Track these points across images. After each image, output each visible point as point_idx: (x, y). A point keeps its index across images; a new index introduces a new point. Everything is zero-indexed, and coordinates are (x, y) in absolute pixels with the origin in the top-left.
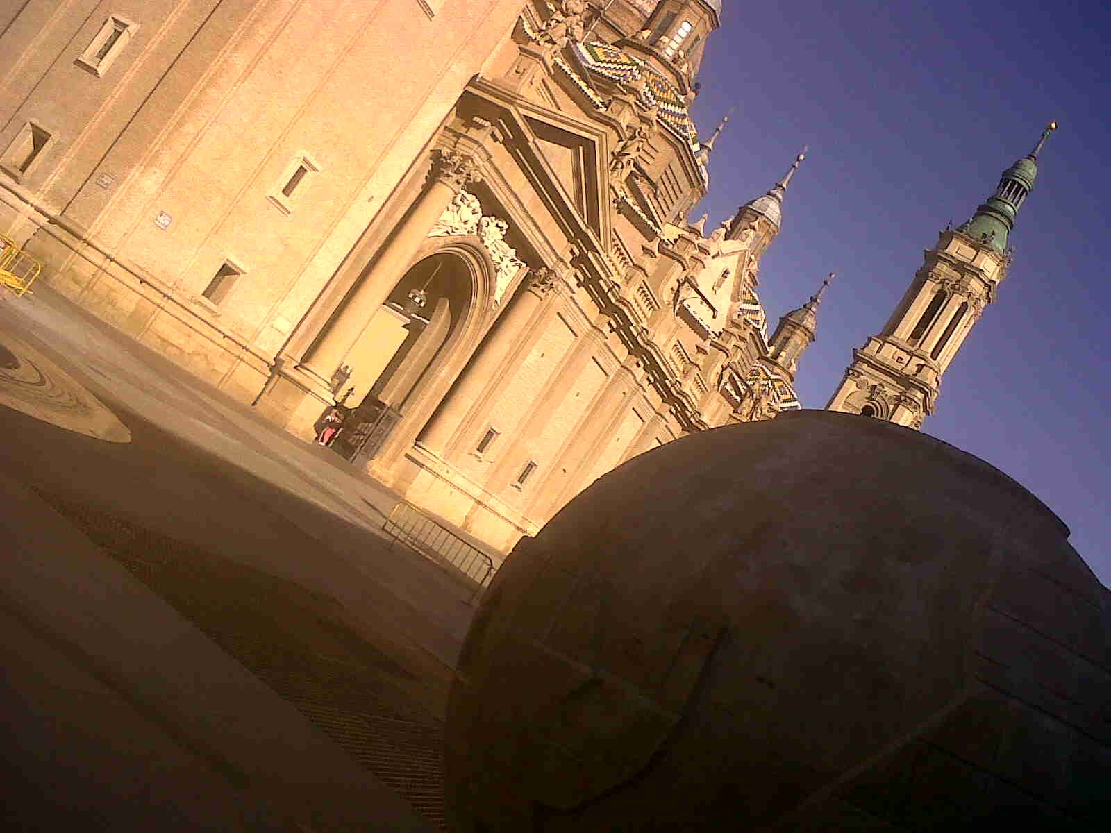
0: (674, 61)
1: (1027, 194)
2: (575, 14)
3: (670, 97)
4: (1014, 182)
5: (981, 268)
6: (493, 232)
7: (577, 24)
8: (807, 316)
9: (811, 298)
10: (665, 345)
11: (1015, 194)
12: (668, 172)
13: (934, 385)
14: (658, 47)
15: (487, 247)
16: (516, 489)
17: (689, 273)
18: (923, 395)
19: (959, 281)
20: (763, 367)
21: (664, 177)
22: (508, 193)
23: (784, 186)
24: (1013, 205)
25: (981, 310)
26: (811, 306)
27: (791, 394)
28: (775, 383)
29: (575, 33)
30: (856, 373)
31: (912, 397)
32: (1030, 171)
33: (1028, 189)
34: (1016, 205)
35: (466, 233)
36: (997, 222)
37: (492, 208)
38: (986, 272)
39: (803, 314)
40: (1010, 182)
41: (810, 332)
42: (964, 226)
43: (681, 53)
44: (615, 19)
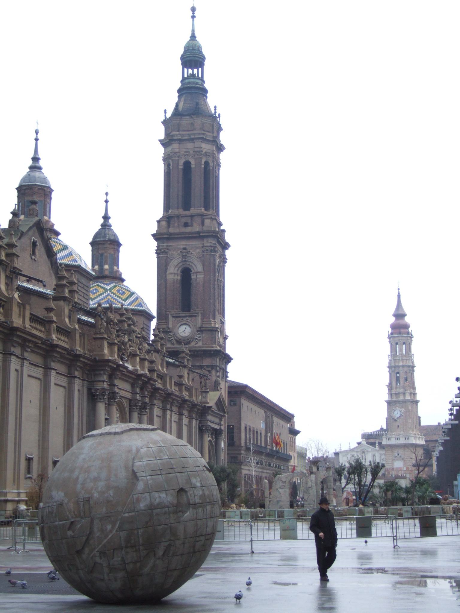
8: (107, 231)
18: (216, 239)
23: (37, 156)
28: (113, 291)
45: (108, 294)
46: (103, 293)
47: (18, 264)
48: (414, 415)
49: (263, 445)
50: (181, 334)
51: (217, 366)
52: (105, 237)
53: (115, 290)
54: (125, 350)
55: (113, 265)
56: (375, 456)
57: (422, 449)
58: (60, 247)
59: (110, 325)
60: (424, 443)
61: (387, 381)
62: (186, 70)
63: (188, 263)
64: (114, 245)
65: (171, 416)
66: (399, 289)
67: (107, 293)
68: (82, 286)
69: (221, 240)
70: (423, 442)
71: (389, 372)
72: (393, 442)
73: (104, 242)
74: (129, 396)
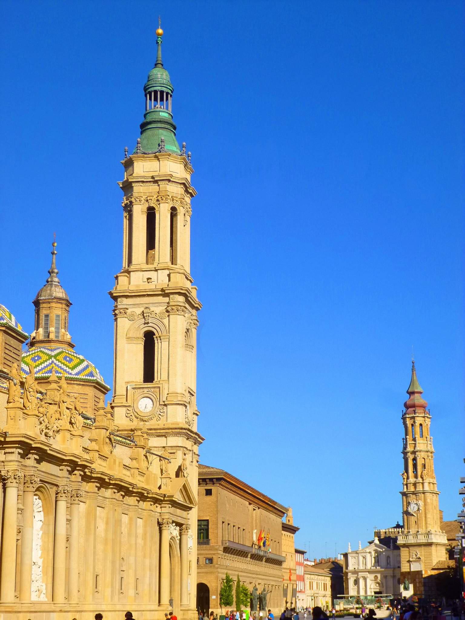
1: (171, 96)
4: (156, 92)
8: (53, 288)
9: (49, 272)
13: (188, 285)
19: (158, 192)
24: (165, 110)
25: (189, 206)
26: (52, 279)
27: (77, 358)
30: (121, 310)
31: (176, 304)
33: (170, 92)
34: (167, 108)
36: (161, 131)
38: (174, 175)
39: (49, 288)
40: (153, 94)
41: (63, 300)
45: (53, 362)
46: (46, 361)
48: (434, 508)
50: (141, 410)
52: (51, 295)
53: (60, 357)
55: (60, 328)
56: (390, 558)
57: (445, 549)
59: (29, 392)
60: (446, 542)
63: (149, 325)
64: (62, 303)
67: (51, 360)
69: (191, 298)
71: (404, 458)
72: (411, 540)
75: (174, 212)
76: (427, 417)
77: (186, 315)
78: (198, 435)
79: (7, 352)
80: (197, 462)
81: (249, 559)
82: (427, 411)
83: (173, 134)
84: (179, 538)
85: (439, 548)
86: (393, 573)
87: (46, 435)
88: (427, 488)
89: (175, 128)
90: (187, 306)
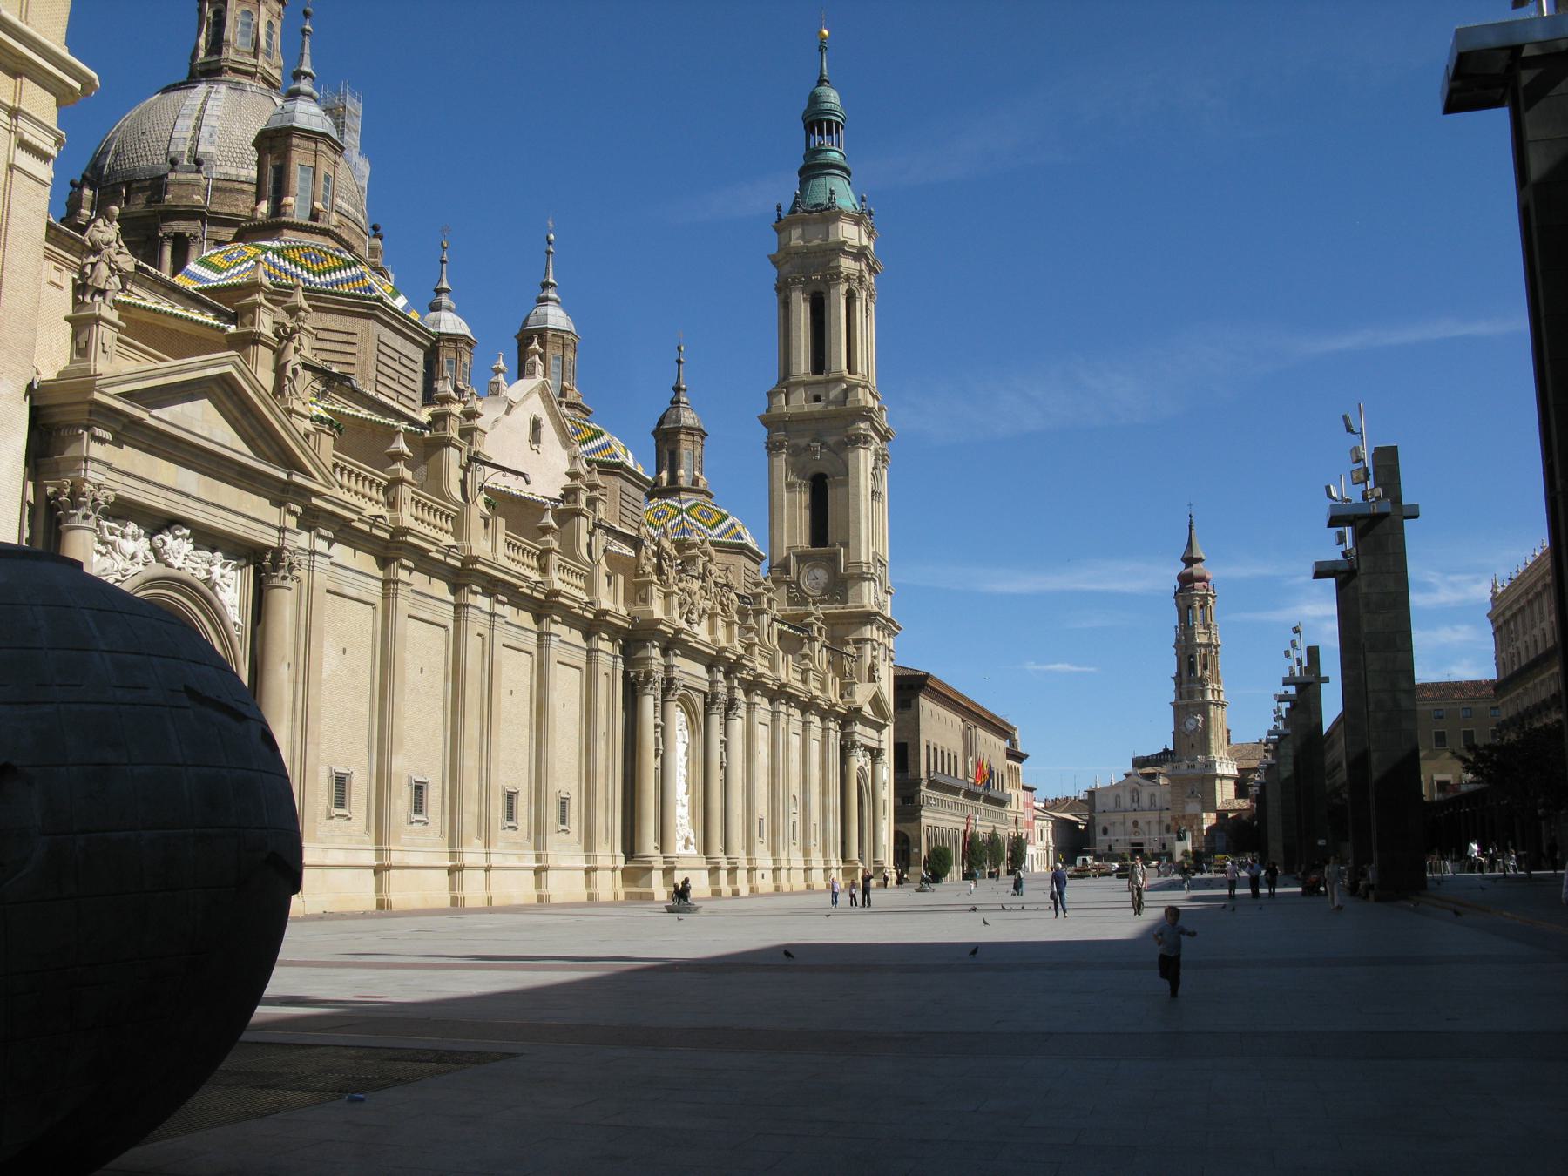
0: (314, 216)
2: (108, 243)
3: (332, 263)
5: (842, 239)
6: (179, 548)
7: (119, 253)
9: (673, 389)
10: (494, 549)
11: (830, 133)
12: (382, 348)
14: (284, 214)
15: (179, 569)
16: (420, 824)
17: (469, 450)
18: (868, 423)
20: (668, 501)
21: (382, 357)
22: (163, 493)
23: (551, 280)
24: (836, 149)
29: (122, 266)
32: (832, 99)
33: (840, 121)
35: (141, 567)
37: (158, 523)
38: (850, 242)
42: (795, 203)
43: (318, 205)
44: (226, 209)
45: (683, 518)
46: (674, 517)
47: (489, 447)
49: (960, 776)
51: (872, 640)
52: (678, 420)
53: (694, 512)
54: (693, 604)
58: (588, 433)
60: (1236, 773)
61: (1174, 671)
62: (812, 137)
64: (693, 435)
65: (788, 723)
66: (1190, 516)
68: (629, 499)
70: (1234, 772)
71: (1176, 654)
73: (677, 431)
74: (705, 687)
75: (851, 298)
76: (1210, 595)
77: (872, 448)
78: (893, 622)
79: (624, 503)
80: (892, 660)
81: (961, 797)
82: (1211, 588)
83: (846, 182)
84: (869, 767)
85: (1224, 781)
86: (1160, 817)
87: (687, 621)
88: (1210, 697)
89: (849, 174)
90: (873, 434)
